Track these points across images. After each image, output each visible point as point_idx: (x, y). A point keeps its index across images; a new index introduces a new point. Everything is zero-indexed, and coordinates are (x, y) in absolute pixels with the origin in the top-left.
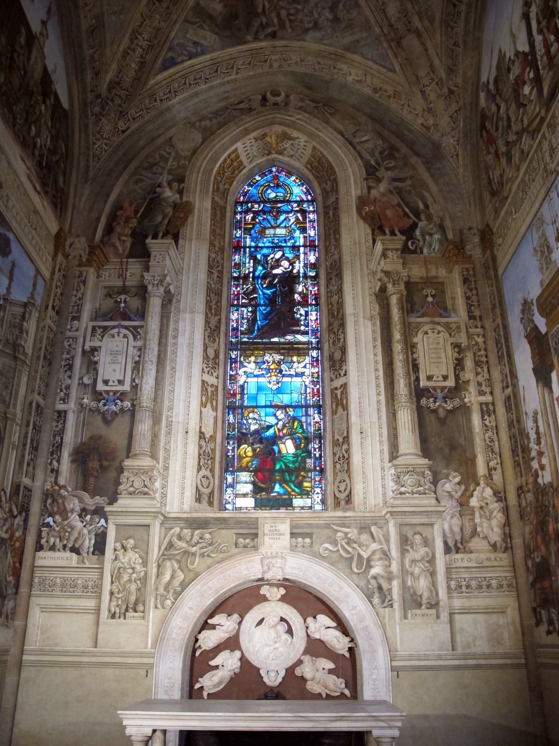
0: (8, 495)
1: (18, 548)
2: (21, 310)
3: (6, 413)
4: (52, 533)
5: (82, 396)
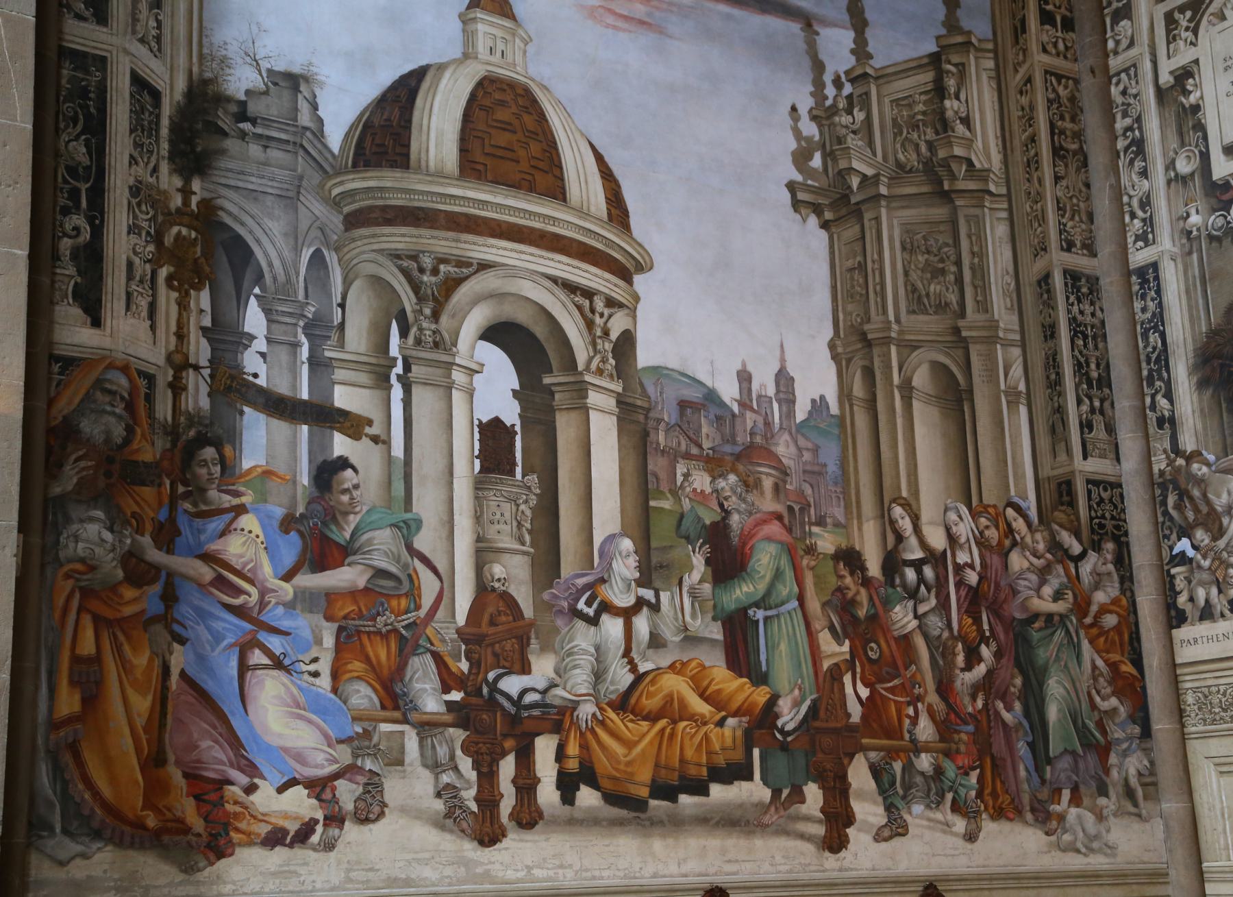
0: (1033, 513)
1: (1117, 628)
2: (929, 76)
3: (957, 331)
4: (1197, 576)
5: (1182, 211)
